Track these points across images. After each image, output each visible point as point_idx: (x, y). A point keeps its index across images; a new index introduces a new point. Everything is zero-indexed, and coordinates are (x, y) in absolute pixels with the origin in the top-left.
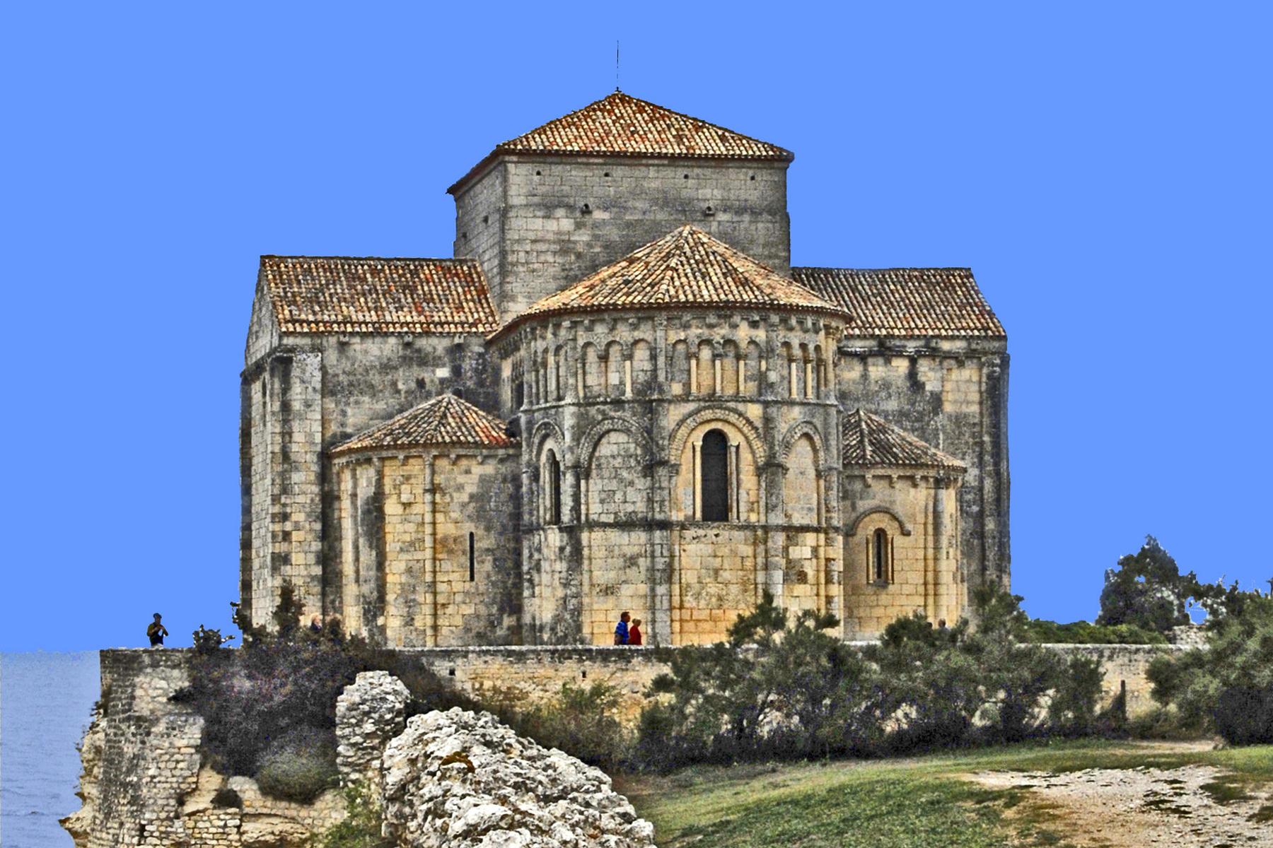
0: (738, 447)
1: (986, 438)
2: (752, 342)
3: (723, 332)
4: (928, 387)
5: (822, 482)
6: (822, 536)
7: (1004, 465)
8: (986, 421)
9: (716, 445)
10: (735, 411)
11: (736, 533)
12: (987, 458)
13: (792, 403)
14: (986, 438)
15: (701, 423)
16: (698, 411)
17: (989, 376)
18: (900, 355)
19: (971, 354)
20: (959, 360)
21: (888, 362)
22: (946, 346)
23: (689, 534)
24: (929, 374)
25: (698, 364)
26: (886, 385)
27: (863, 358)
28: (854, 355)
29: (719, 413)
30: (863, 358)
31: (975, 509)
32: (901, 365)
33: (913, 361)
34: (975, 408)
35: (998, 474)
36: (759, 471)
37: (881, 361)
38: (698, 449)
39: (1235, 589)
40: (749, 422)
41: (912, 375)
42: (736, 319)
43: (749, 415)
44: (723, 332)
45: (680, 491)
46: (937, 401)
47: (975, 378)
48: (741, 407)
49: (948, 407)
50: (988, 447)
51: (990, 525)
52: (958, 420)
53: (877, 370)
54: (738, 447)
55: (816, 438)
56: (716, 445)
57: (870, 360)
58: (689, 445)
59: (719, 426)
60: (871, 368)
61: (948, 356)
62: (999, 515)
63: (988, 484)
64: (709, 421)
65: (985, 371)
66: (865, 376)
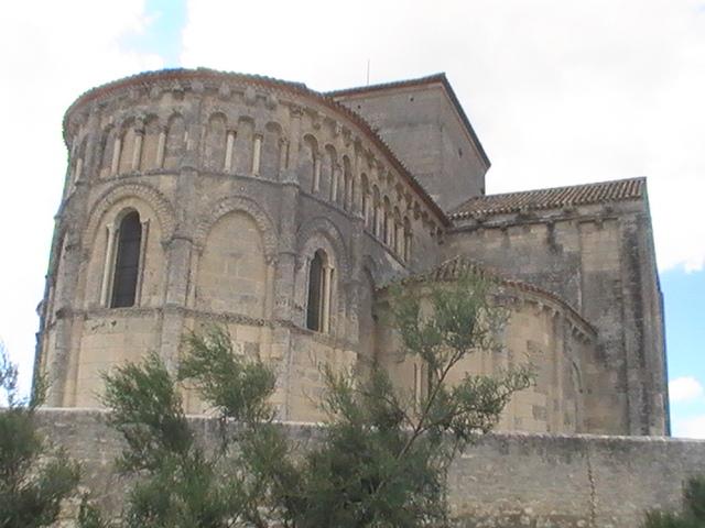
0: (147, 224)
1: (626, 292)
2: (176, 115)
3: (145, 107)
4: (566, 249)
5: (271, 268)
6: (265, 330)
7: (647, 318)
8: (626, 276)
9: (131, 227)
10: (144, 184)
11: (134, 320)
12: (628, 311)
13: (220, 176)
14: (626, 292)
15: (115, 203)
16: (110, 191)
17: (626, 233)
18: (537, 223)
19: (608, 216)
20: (598, 223)
21: (527, 230)
22: (584, 211)
23: (90, 323)
24: (567, 238)
25: (122, 146)
26: (526, 251)
27: (503, 229)
28: (496, 227)
29: (129, 190)
30: (503, 229)
31: (620, 362)
32: (540, 232)
33: (551, 226)
34: (616, 266)
35: (640, 325)
36: (166, 245)
37: (520, 229)
38: (112, 231)
39: (377, 130)
40: (160, 195)
41: (550, 240)
42: (156, 91)
43: (161, 188)
44: (145, 107)
45: (89, 275)
46: (576, 261)
47: (614, 239)
48: (153, 180)
49: (589, 268)
50: (628, 300)
51: (633, 377)
52: (599, 278)
53: (517, 239)
54: (147, 224)
55: (260, 219)
56: (131, 227)
57: (510, 230)
58: (102, 227)
59: (130, 203)
60: (511, 238)
61: (583, 221)
62: (643, 365)
63: (630, 336)
64: (120, 200)
65: (622, 228)
66: (506, 245)
